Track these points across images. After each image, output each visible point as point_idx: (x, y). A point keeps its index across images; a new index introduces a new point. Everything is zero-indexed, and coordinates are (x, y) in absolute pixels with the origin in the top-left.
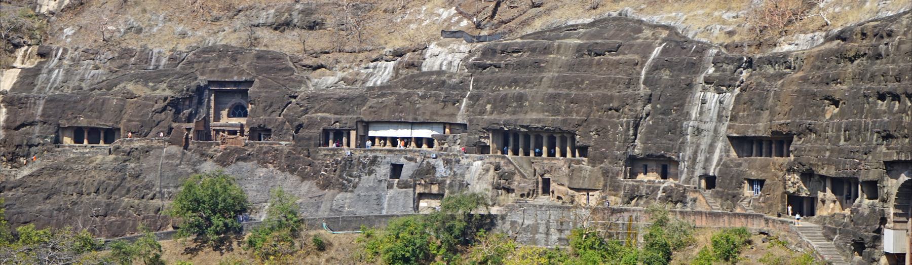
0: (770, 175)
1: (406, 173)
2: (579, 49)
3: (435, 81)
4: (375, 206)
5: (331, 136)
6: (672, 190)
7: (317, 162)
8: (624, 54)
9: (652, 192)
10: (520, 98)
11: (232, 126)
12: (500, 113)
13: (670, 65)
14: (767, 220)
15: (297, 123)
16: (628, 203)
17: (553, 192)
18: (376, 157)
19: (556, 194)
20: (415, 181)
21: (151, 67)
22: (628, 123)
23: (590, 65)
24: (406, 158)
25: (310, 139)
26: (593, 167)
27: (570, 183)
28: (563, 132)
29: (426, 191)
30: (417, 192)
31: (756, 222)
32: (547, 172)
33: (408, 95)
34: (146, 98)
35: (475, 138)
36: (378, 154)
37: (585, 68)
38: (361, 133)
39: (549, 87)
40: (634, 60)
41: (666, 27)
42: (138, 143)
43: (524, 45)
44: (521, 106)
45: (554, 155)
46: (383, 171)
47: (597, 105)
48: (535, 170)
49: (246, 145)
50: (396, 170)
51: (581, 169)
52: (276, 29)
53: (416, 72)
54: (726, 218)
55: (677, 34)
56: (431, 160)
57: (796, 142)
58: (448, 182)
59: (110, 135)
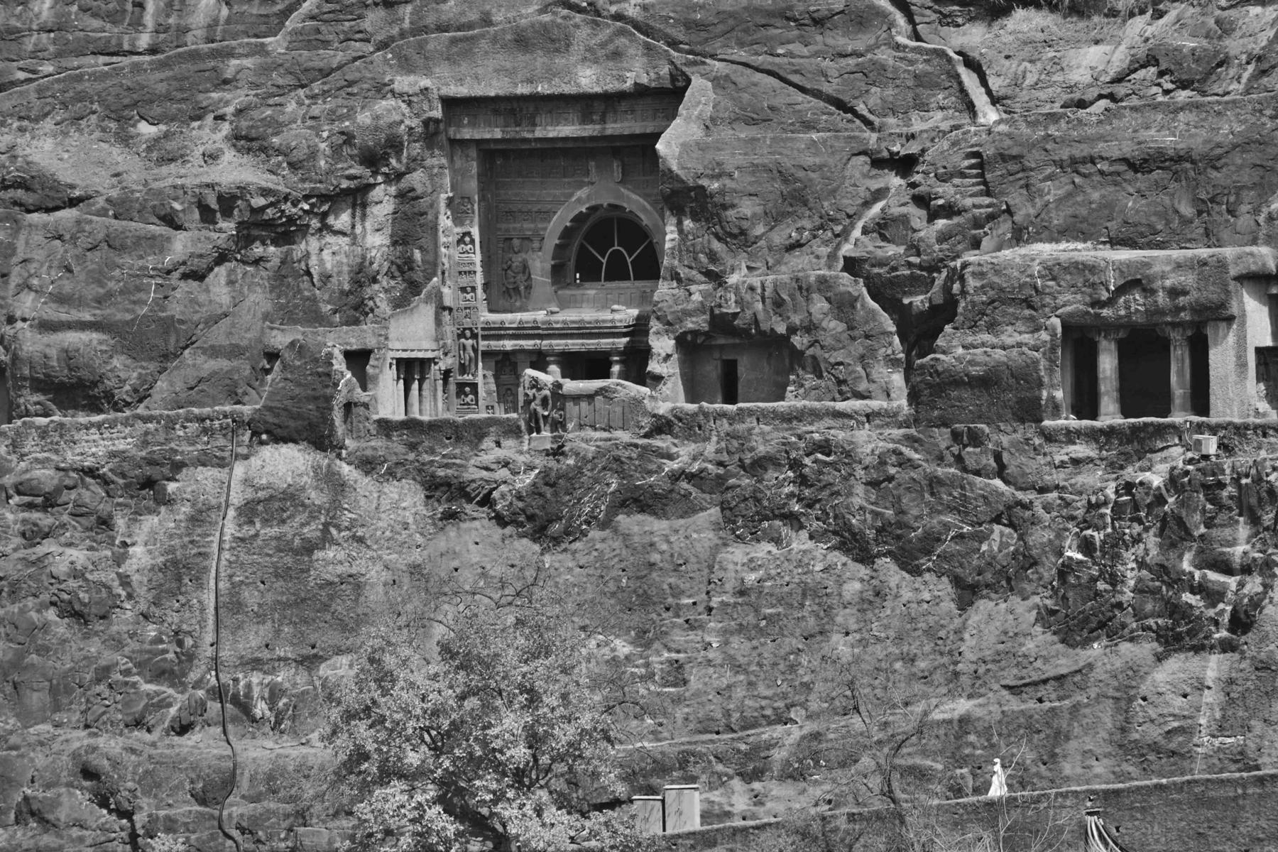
5: (1107, 364)
15: (918, 301)
21: (144, 41)
25: (987, 382)
34: (121, 208)
42: (97, 441)
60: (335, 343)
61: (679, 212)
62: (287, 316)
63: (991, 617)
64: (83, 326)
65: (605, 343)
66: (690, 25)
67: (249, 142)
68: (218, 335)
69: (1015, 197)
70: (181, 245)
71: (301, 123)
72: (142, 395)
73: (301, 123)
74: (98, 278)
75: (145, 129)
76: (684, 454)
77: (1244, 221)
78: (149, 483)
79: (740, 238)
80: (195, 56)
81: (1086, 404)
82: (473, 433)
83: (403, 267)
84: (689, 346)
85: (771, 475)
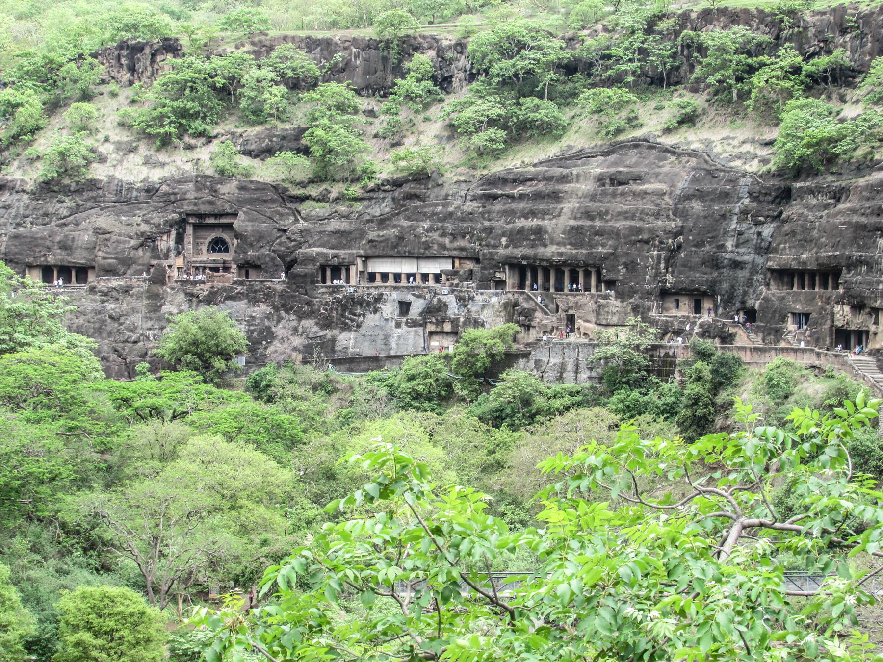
0: (817, 308)
1: (415, 311)
2: (600, 179)
3: (441, 212)
5: (328, 273)
6: (710, 326)
7: (315, 301)
10: (539, 231)
11: (215, 262)
12: (515, 247)
13: (700, 195)
14: (818, 354)
15: (289, 259)
16: (662, 339)
18: (382, 294)
19: (582, 331)
22: (659, 256)
23: (614, 195)
24: (414, 295)
25: (305, 275)
27: (598, 319)
28: (586, 265)
29: (438, 330)
30: (428, 330)
31: (806, 356)
32: (570, 308)
33: (413, 228)
36: (382, 291)
37: (609, 198)
41: (693, 154)
42: (116, 282)
43: (538, 173)
44: (540, 239)
46: (389, 309)
47: (625, 238)
48: (558, 306)
50: (405, 307)
52: (256, 156)
53: (419, 203)
54: (773, 352)
55: (706, 162)
56: (441, 297)
57: (846, 276)
58: (462, 320)
59: (82, 272)
60: (165, 263)
62: (154, 258)
67: (147, 222)
68: (140, 262)
70: (133, 243)
71: (157, 218)
72: (124, 273)
73: (157, 218)
74: (115, 249)
76: (239, 288)
79: (251, 245)
81: (324, 281)
83: (177, 248)
84: (240, 267)
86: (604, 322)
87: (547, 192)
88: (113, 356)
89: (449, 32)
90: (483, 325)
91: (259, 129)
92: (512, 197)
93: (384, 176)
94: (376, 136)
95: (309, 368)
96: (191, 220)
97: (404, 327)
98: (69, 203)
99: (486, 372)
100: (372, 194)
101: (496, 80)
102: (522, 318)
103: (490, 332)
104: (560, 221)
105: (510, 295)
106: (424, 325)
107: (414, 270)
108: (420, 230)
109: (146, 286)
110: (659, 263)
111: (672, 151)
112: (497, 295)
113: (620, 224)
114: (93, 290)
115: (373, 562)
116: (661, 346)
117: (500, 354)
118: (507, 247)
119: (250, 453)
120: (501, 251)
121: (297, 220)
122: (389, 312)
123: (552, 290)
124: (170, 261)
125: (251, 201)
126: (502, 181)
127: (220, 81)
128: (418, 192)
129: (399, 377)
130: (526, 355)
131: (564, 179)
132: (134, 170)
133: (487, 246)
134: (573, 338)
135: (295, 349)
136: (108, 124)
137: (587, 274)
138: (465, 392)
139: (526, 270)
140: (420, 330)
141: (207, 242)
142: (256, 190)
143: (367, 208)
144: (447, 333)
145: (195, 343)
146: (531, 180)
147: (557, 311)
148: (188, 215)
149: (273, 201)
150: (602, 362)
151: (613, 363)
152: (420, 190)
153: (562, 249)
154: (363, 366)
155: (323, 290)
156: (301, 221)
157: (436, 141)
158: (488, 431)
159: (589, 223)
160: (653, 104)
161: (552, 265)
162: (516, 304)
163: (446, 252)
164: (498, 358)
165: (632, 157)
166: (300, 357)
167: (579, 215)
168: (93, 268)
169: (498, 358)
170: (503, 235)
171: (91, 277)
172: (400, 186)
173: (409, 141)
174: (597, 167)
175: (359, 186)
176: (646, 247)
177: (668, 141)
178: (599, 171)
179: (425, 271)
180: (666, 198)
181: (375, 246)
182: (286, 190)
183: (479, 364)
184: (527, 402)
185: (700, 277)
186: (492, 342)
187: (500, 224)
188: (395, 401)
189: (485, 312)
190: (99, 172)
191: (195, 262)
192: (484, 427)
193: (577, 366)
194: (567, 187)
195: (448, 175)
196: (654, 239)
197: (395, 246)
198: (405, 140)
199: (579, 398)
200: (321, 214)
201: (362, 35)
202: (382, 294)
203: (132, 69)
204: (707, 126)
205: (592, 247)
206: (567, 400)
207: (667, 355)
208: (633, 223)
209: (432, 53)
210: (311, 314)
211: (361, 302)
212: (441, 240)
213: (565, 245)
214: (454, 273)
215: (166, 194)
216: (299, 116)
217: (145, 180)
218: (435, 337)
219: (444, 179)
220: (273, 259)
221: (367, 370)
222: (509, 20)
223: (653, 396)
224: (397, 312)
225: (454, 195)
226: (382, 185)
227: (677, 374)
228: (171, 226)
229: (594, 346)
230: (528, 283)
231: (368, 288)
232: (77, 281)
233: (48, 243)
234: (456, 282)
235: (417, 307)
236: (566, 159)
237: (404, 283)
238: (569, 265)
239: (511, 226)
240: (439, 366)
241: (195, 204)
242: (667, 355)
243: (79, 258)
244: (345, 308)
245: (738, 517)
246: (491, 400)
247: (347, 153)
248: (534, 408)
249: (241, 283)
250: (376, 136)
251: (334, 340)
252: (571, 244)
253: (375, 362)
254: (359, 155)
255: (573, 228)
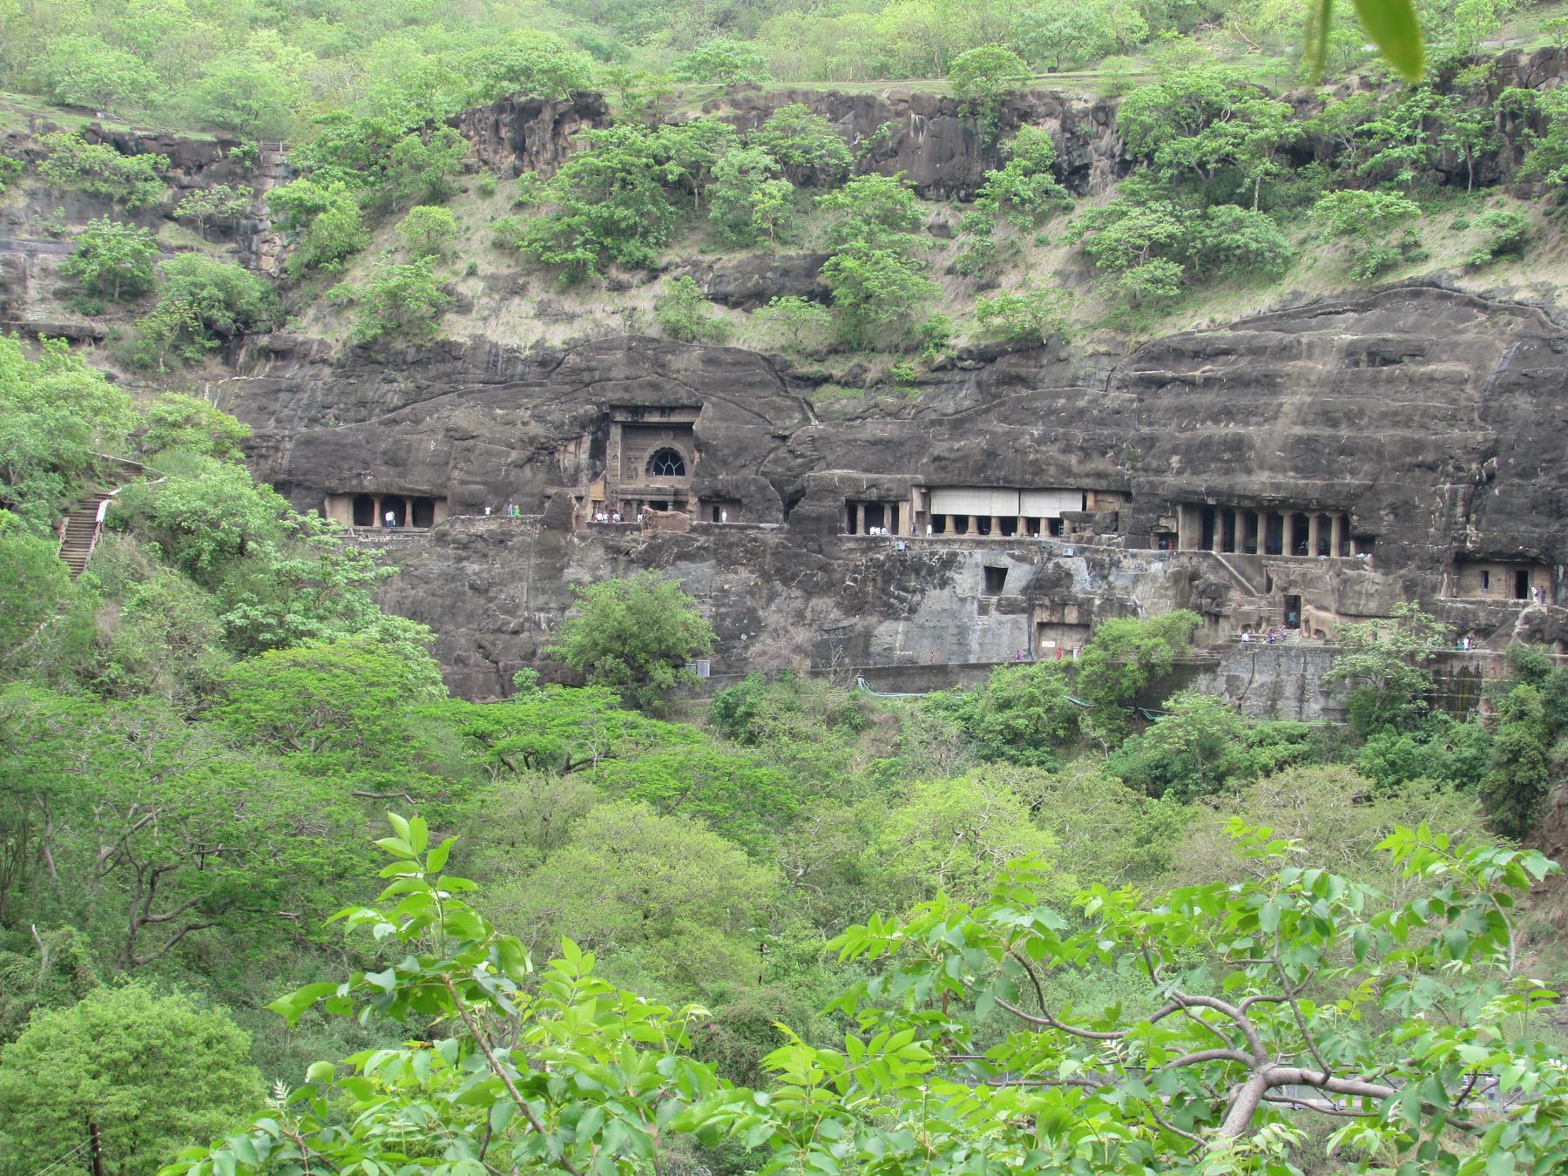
2: (1350, 353)
3: (1063, 409)
4: (955, 648)
5: (861, 515)
6: (1543, 619)
7: (836, 563)
8: (1441, 361)
9: (1503, 622)
10: (1237, 445)
12: (1195, 472)
13: (1530, 384)
15: (790, 489)
17: (1307, 622)
18: (955, 554)
19: (1313, 626)
20: (1030, 599)
22: (1454, 493)
23: (1374, 382)
24: (1012, 556)
25: (819, 519)
26: (1386, 574)
27: (1341, 604)
28: (1322, 507)
29: (1055, 619)
30: (1037, 620)
32: (1292, 583)
35: (1148, 520)
36: (956, 548)
38: (918, 505)
39: (1295, 423)
40: (1460, 372)
41: (1519, 309)
43: (1238, 341)
44: (1241, 459)
45: (1305, 552)
46: (968, 581)
47: (1392, 459)
48: (1270, 581)
49: (694, 529)
50: (995, 577)
51: (1360, 580)
52: (735, 305)
53: (1025, 392)
55: (1542, 324)
56: (1061, 561)
58: (1097, 602)
59: (423, 507)
60: (572, 493)
61: (700, 451)
62: (552, 483)
63: (820, 603)
64: (477, 483)
65: (666, 498)
66: (703, 384)
67: (540, 418)
68: (528, 489)
69: (827, 453)
70: (514, 455)
71: (557, 413)
73: (557, 413)
75: (499, 411)
76: (702, 540)
77: (912, 466)
78: (502, 542)
79: (725, 463)
80: (517, 385)
81: (853, 530)
82: (621, 529)
83: (593, 467)
84: (703, 502)
85: (735, 549)
86: (1353, 610)
87: (1251, 372)
88: (476, 657)
89: (1085, 87)
90: (1135, 613)
91: (741, 255)
92: (1191, 383)
93: (963, 342)
94: (950, 271)
95: (821, 683)
96: (619, 417)
97: (994, 614)
98: (403, 383)
99: (1139, 697)
100: (940, 375)
101: (1166, 173)
102: (1205, 601)
103: (1147, 624)
104: (1277, 426)
105: (1184, 560)
106: (1029, 610)
107: (1013, 512)
108: (1026, 440)
109: (536, 532)
110: (1453, 505)
111: (1480, 303)
112: (1160, 558)
113: (1384, 435)
114: (442, 538)
115: (441, 1143)
116: (1454, 656)
117: (1163, 665)
118: (1180, 472)
119: (701, 836)
120: (1170, 479)
121: (806, 420)
122: (967, 586)
123: (1260, 552)
124: (581, 490)
125: (726, 385)
126: (1176, 353)
127: (674, 170)
128: (1023, 371)
129: (982, 703)
130: (1211, 668)
131: (1285, 352)
132: (519, 328)
133: (1145, 470)
134: (1296, 638)
135: (798, 649)
136: (475, 245)
137: (1324, 524)
138: (1100, 733)
139: (1215, 516)
140: (1023, 618)
141: (647, 455)
142: (736, 364)
143: (932, 399)
144: (1071, 626)
145: (621, 636)
146: (1226, 352)
147: (1269, 589)
148: (613, 407)
149: (764, 384)
150: (1347, 681)
151: (1368, 685)
152: (1027, 369)
153: (1280, 478)
154: (920, 682)
155: (851, 545)
156: (815, 422)
157: (1058, 280)
158: (1140, 802)
159: (1327, 432)
160: (1448, 219)
161: (1260, 507)
162: (1194, 576)
163: (1071, 480)
164: (1160, 672)
165: (1409, 314)
166: (808, 663)
167: (1310, 418)
168: (443, 499)
169: (1160, 672)
170: (1175, 451)
171: (440, 516)
172: (992, 360)
173: (1009, 280)
174: (1345, 332)
175: (918, 360)
176: (1431, 476)
177: (1474, 286)
178: (1348, 337)
179: (1031, 512)
180: (1469, 388)
181: (944, 468)
182: (788, 365)
183: (1125, 683)
184: (1210, 751)
185: (1527, 533)
186: (1151, 643)
187: (1169, 431)
188: (973, 747)
189: (1139, 588)
190: (458, 330)
191: (624, 492)
192: (1133, 795)
193: (1302, 689)
194: (1290, 366)
195: (1077, 342)
196: (1445, 463)
197: (981, 468)
198: (1003, 279)
199: (1302, 747)
200: (850, 409)
201: (928, 90)
202: (955, 554)
203: (519, 148)
204: (1544, 260)
205: (1332, 474)
206: (1283, 750)
207: (1464, 671)
208: (1407, 433)
209: (1053, 124)
210: (828, 588)
211: (917, 567)
212: (1062, 458)
213: (1284, 471)
214: (1084, 518)
215: (575, 371)
216: (814, 234)
217: (537, 345)
218: (1050, 633)
219: (1071, 349)
220: (762, 489)
221: (926, 690)
222: (1192, 66)
223: (1437, 744)
224: (982, 585)
225: (1086, 378)
226: (960, 358)
227: (1482, 707)
228: (583, 427)
229: (1333, 653)
230: (1217, 538)
231: (931, 543)
232: (415, 523)
233: (365, 454)
234: (1088, 534)
235: (1017, 577)
236: (1289, 316)
237: (995, 534)
238: (1292, 506)
239: (1188, 434)
240: (1054, 685)
241: (627, 389)
242: (1464, 671)
243: (419, 482)
244: (888, 577)
245: (1259, 1062)
246: (1147, 746)
247: (897, 301)
248: (1222, 763)
249: (705, 530)
250: (950, 271)
251: (868, 635)
252: (1296, 469)
253: (940, 674)
254: (917, 306)
255: (1299, 440)
